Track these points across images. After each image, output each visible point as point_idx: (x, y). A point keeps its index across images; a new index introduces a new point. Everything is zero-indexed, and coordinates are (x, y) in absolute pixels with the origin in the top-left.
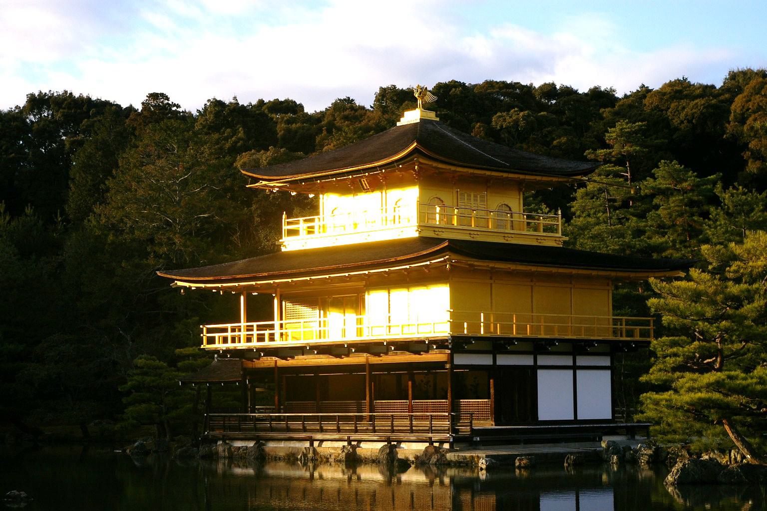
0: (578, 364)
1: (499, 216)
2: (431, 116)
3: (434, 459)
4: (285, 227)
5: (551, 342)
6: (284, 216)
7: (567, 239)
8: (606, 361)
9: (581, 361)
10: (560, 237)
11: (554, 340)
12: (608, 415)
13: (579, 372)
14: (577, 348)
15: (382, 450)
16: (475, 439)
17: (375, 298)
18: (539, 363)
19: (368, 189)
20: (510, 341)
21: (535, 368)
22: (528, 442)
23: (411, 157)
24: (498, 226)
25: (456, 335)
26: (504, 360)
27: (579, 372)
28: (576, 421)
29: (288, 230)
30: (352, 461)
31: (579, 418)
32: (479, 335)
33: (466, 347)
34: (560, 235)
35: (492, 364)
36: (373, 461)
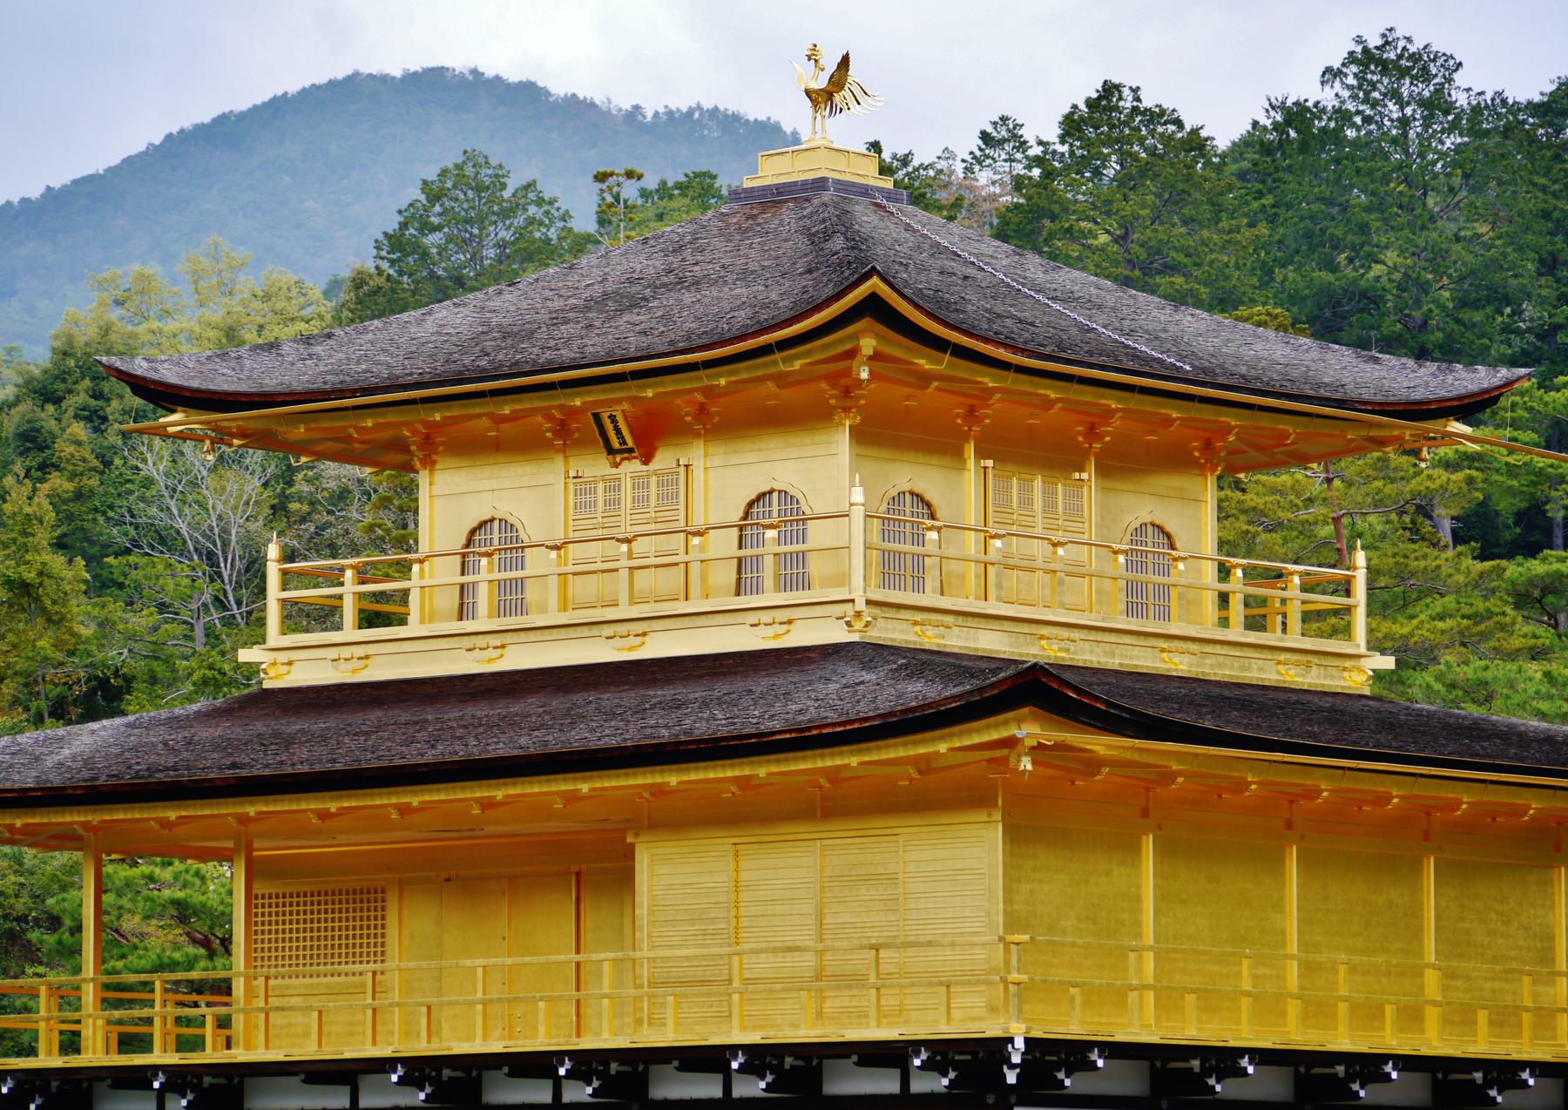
6: (273, 551)
7: (1388, 663)
10: (1359, 657)
11: (1385, 1058)
19: (631, 450)
23: (850, 329)
24: (1130, 610)
25: (1037, 1034)
32: (1119, 1038)
33: (1067, 1082)
34: (1363, 650)
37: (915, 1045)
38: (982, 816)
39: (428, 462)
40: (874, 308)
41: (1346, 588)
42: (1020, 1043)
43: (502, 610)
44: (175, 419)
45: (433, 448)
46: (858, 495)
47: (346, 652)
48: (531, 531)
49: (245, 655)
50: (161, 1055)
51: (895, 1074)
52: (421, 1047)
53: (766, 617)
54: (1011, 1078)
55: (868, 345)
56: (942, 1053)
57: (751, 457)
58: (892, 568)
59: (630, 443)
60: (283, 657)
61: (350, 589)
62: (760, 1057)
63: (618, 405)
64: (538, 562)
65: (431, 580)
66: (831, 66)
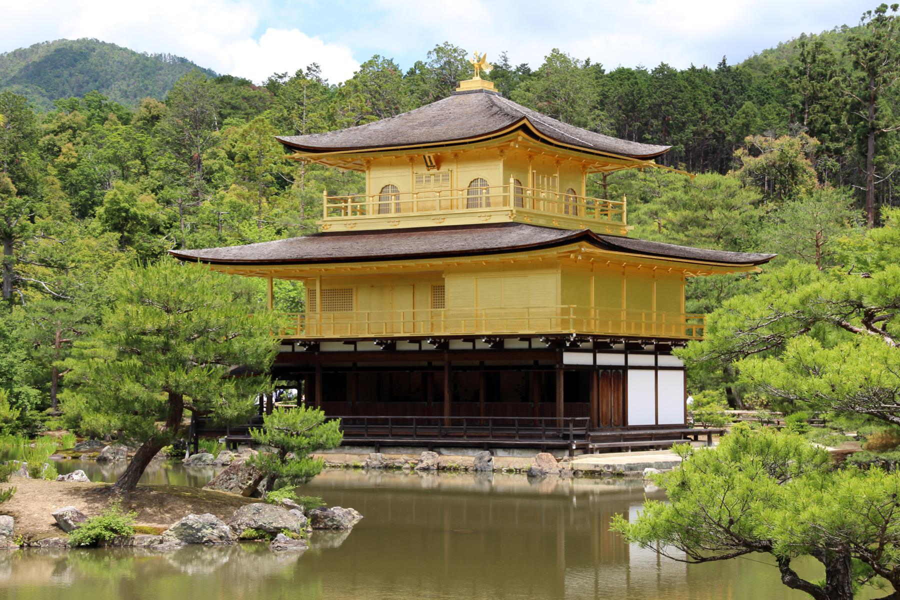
0: (660, 363)
2: (490, 86)
9: (663, 360)
12: (681, 421)
13: (659, 372)
16: (591, 446)
17: (458, 289)
18: (630, 363)
20: (616, 339)
21: (625, 368)
22: (635, 449)
26: (604, 359)
27: (659, 372)
28: (657, 427)
29: (328, 208)
31: (659, 423)
36: (466, 470)
37: (540, 336)
38: (555, 271)
39: (368, 168)
40: (524, 128)
41: (620, 206)
42: (574, 335)
43: (398, 210)
44: (297, 155)
45: (369, 164)
46: (512, 180)
47: (349, 222)
48: (401, 189)
49: (318, 222)
51: (527, 343)
52: (384, 334)
53: (483, 214)
54: (568, 344)
55: (520, 139)
56: (547, 337)
57: (471, 169)
58: (520, 202)
59: (434, 164)
60: (329, 223)
62: (489, 338)
63: (430, 154)
64: (403, 199)
65: (371, 202)
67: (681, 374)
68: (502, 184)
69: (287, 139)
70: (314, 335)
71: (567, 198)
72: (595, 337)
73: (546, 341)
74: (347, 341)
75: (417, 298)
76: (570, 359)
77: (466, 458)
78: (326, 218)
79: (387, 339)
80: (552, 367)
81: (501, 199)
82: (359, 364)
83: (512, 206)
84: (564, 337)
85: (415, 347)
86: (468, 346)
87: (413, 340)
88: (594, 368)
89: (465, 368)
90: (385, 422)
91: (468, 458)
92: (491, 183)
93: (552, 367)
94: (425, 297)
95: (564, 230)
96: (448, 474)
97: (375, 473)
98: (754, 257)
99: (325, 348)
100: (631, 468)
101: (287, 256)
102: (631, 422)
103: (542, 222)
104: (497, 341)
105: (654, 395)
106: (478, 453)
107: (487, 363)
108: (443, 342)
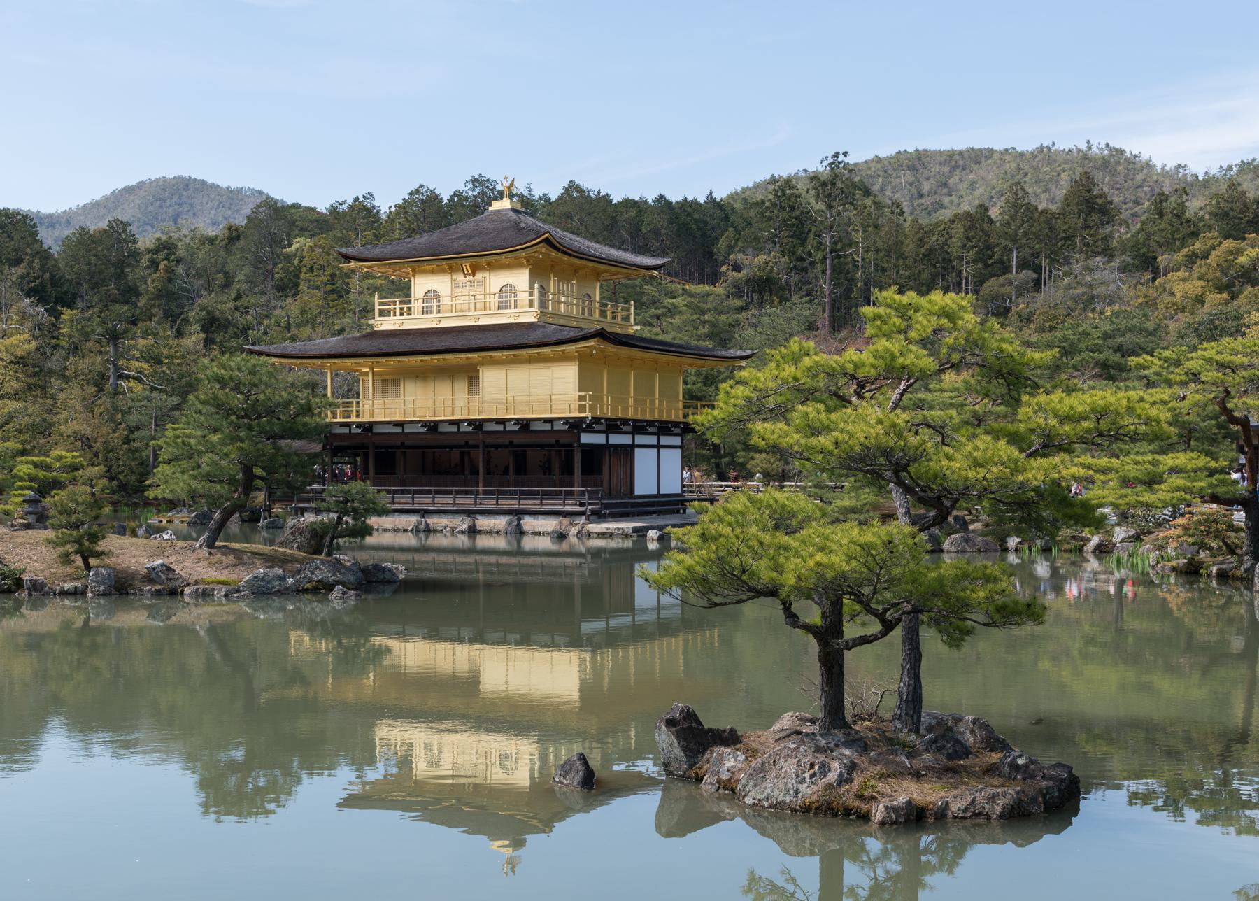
1: (574, 303)
3: (574, 531)
4: (377, 308)
5: (651, 423)
8: (677, 441)
9: (665, 440)
12: (679, 491)
14: (664, 428)
15: (510, 523)
20: (625, 422)
21: (633, 446)
26: (615, 439)
28: (659, 495)
30: (473, 531)
35: (604, 442)
36: (497, 532)
40: (547, 241)
41: (629, 310)
43: (439, 312)
45: (415, 272)
48: (442, 293)
50: (354, 419)
56: (567, 421)
58: (543, 304)
61: (398, 306)
62: (518, 421)
64: (445, 301)
65: (416, 305)
66: (510, 181)
67: (679, 451)
68: (527, 288)
69: (344, 250)
70: (366, 418)
71: (584, 302)
72: (607, 419)
73: (566, 423)
74: (396, 424)
75: (456, 386)
76: (586, 438)
77: (498, 522)
78: (377, 318)
79: (430, 421)
80: (571, 445)
81: (527, 302)
82: (407, 443)
83: (536, 309)
84: (582, 420)
85: (454, 429)
86: (500, 428)
87: (452, 423)
88: (607, 446)
89: (497, 447)
90: (429, 492)
91: (501, 522)
92: (519, 288)
93: (571, 445)
94: (462, 387)
95: (582, 329)
96: (483, 536)
97: (422, 536)
98: (739, 353)
99: (377, 430)
100: (635, 530)
101: (345, 351)
102: (638, 491)
103: (562, 322)
104: (525, 424)
105: (659, 470)
106: (508, 518)
107: (516, 441)
108: (478, 425)
